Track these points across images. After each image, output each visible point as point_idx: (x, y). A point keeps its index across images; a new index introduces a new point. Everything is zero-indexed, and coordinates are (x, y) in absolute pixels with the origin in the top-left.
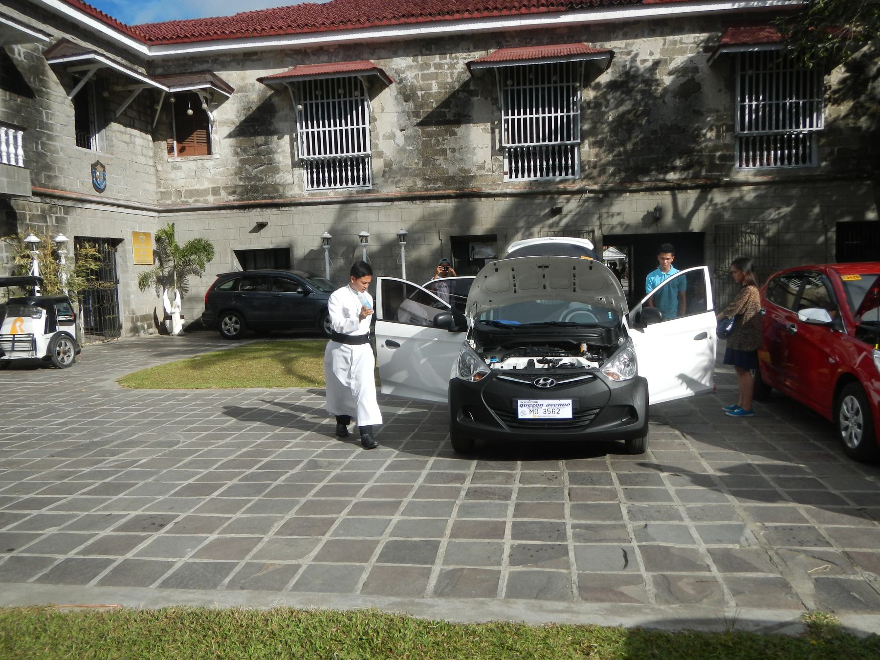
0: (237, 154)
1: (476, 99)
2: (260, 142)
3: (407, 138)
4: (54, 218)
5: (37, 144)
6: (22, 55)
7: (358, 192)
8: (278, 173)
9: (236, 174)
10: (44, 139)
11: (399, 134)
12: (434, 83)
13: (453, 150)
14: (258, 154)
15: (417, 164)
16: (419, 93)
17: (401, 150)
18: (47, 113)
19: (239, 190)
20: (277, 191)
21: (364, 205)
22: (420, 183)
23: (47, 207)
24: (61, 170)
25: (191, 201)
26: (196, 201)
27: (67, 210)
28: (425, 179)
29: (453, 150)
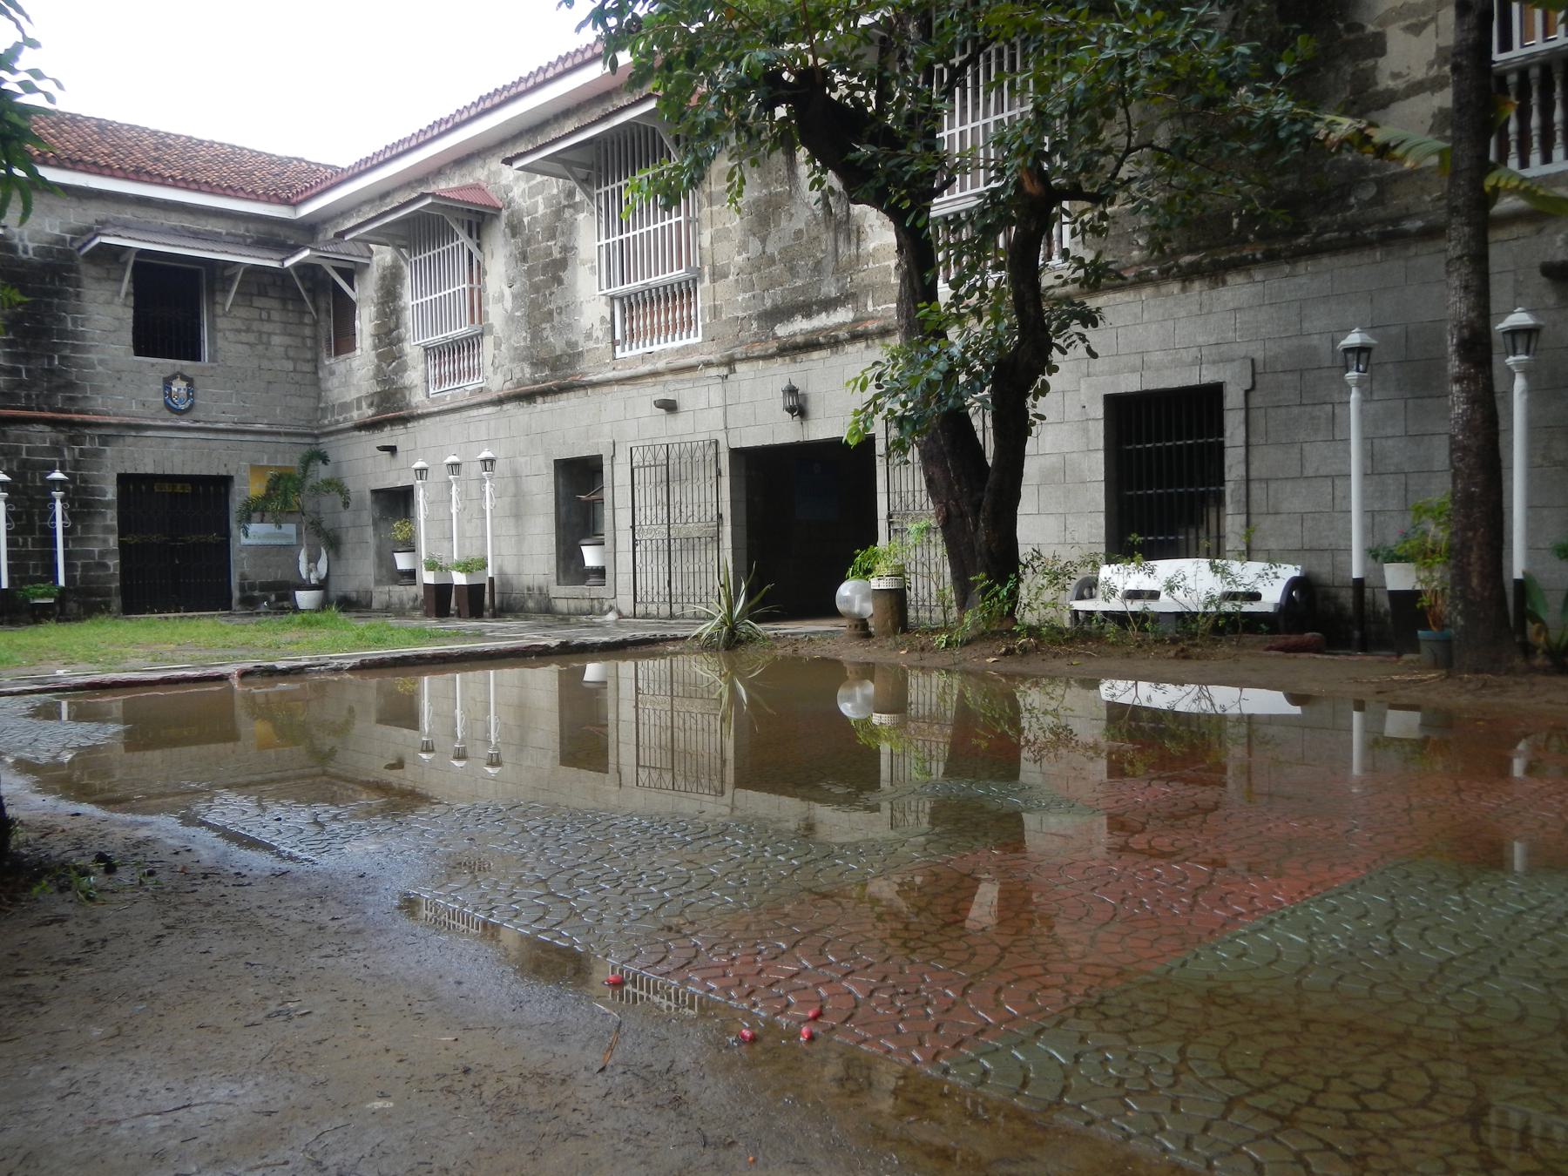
0: (375, 347)
1: (581, 217)
2: (392, 326)
3: (515, 297)
4: (77, 451)
5: (51, 358)
6: (31, 252)
7: (472, 393)
8: (405, 371)
9: (375, 376)
10: (67, 352)
11: (507, 292)
12: (540, 199)
13: (560, 310)
14: (391, 344)
15: (525, 338)
16: (526, 220)
17: (510, 319)
18: (75, 321)
19: (376, 400)
20: (405, 397)
21: (474, 412)
22: (528, 371)
23: (62, 437)
24: (97, 390)
25: (341, 418)
26: (345, 420)
27: (105, 440)
28: (533, 364)
29: (560, 310)
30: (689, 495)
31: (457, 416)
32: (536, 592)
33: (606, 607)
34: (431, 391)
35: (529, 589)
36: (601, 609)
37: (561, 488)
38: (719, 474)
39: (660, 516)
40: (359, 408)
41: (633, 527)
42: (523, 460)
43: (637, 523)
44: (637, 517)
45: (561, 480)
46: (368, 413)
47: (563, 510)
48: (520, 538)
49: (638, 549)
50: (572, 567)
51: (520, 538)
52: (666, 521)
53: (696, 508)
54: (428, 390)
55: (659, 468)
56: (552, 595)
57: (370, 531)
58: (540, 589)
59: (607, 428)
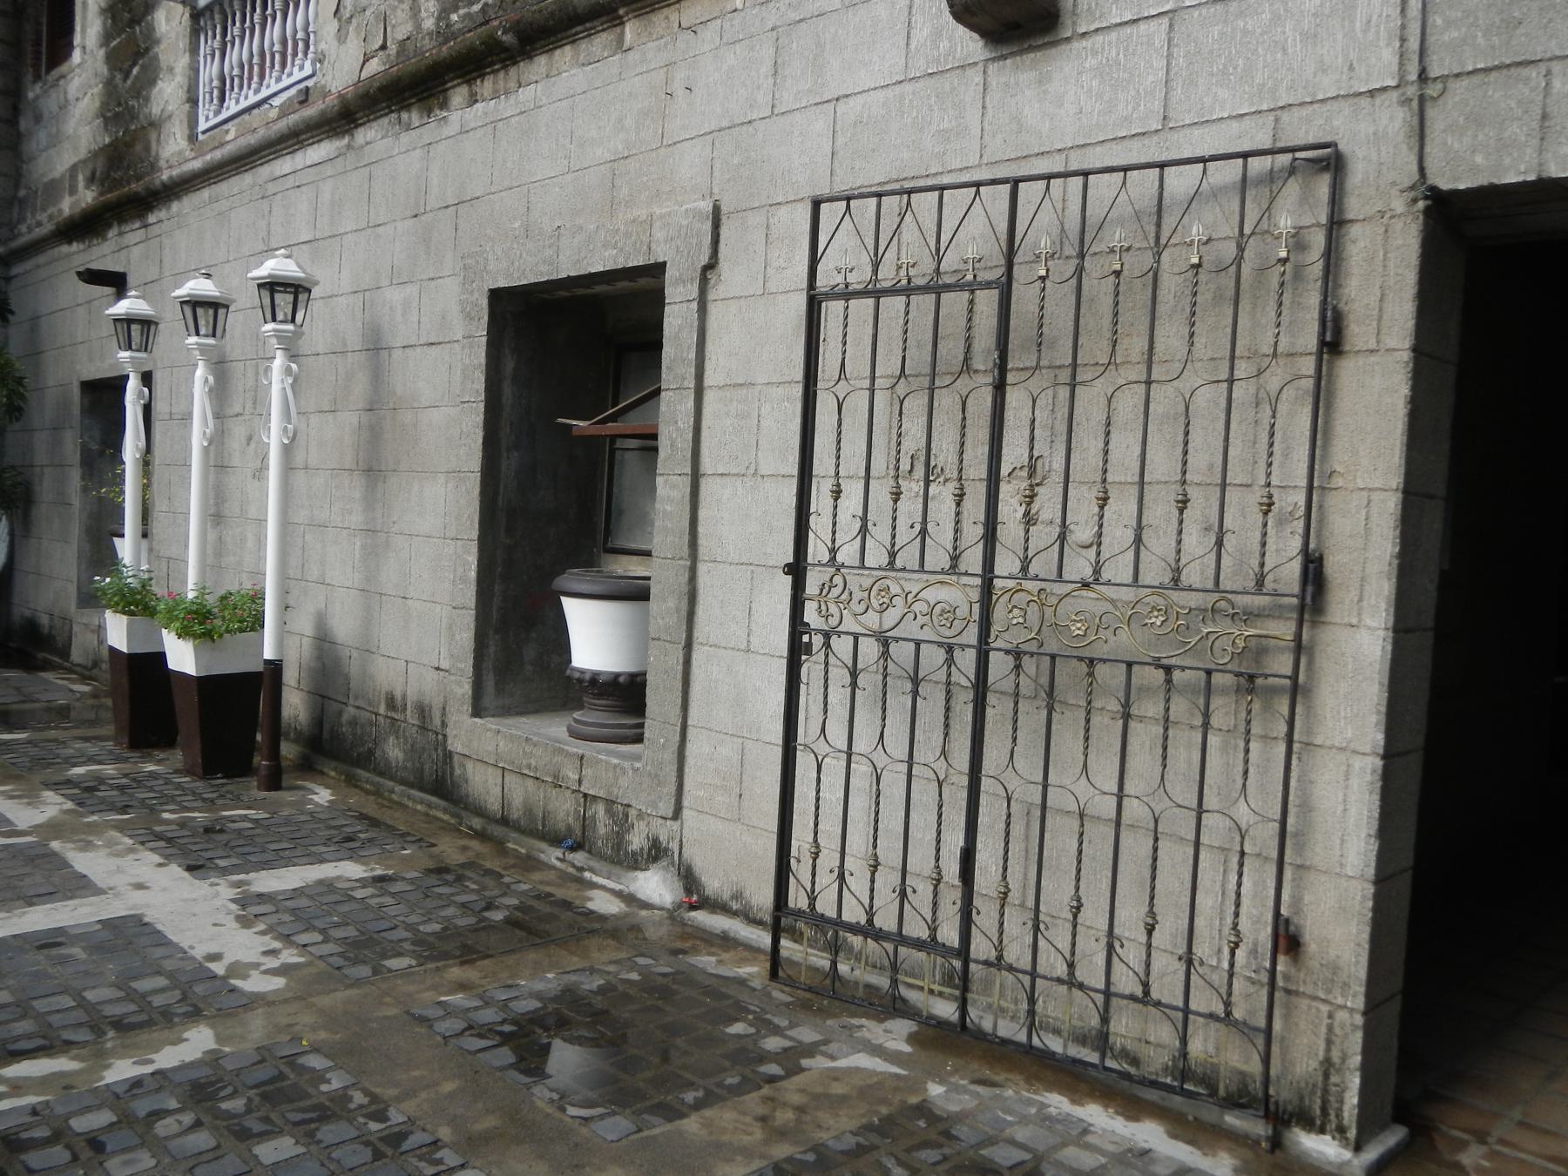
7: (285, 111)
21: (284, 165)
30: (1125, 447)
31: (243, 182)
32: (412, 717)
33: (637, 841)
34: (202, 126)
35: (391, 703)
36: (619, 840)
37: (508, 390)
38: (1332, 344)
39: (942, 534)
40: (73, 190)
41: (797, 570)
42: (395, 295)
43: (817, 550)
44: (819, 525)
45: (509, 365)
46: (87, 197)
47: (509, 464)
48: (375, 541)
49: (811, 670)
50: (530, 653)
51: (375, 541)
52: (973, 560)
53: (1160, 511)
54: (193, 121)
55: (954, 303)
56: (456, 745)
57: (75, 478)
58: (423, 711)
59: (689, 164)
